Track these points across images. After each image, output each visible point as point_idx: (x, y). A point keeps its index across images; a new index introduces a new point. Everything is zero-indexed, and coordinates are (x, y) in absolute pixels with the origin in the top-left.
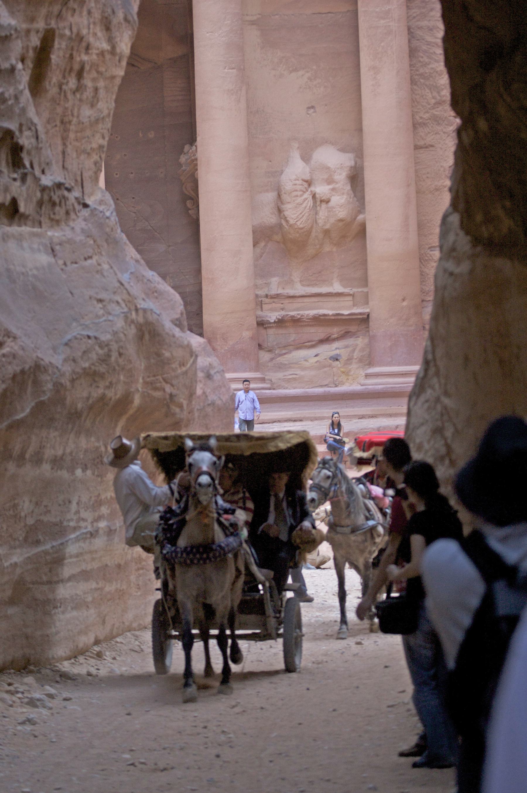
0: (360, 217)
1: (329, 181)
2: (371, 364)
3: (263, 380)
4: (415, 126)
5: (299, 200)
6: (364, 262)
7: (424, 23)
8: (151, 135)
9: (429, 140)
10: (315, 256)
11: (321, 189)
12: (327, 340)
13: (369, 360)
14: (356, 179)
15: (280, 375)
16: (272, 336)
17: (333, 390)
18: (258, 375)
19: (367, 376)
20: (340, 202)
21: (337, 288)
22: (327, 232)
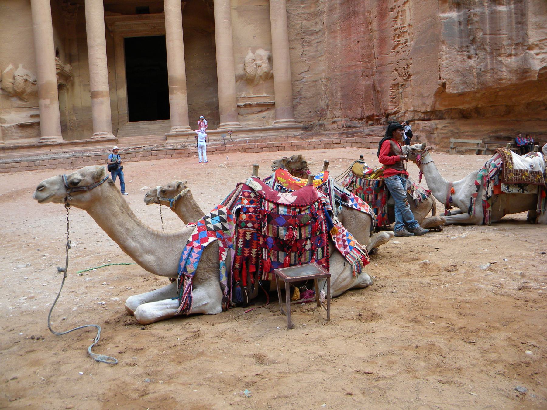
0: (272, 71)
1: (261, 59)
2: (276, 119)
3: (240, 125)
4: (289, 41)
5: (251, 65)
6: (273, 87)
7: (292, 8)
8: (208, 54)
9: (294, 46)
10: (257, 85)
11: (259, 62)
12: (261, 111)
13: (275, 117)
14: (270, 59)
15: (245, 123)
16: (243, 110)
17: (263, 127)
18: (238, 123)
19: (275, 123)
20: (265, 67)
21: (265, 95)
22: (261, 76)
